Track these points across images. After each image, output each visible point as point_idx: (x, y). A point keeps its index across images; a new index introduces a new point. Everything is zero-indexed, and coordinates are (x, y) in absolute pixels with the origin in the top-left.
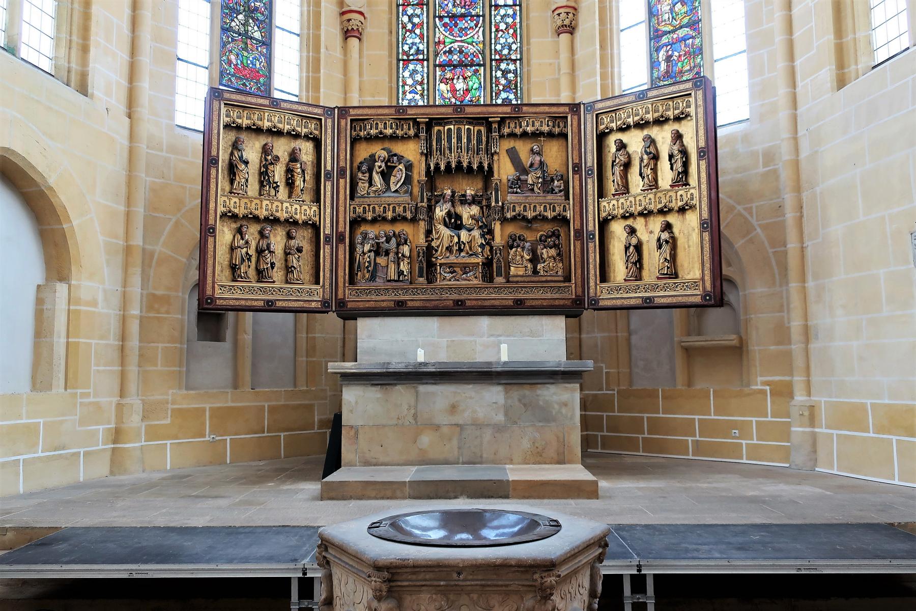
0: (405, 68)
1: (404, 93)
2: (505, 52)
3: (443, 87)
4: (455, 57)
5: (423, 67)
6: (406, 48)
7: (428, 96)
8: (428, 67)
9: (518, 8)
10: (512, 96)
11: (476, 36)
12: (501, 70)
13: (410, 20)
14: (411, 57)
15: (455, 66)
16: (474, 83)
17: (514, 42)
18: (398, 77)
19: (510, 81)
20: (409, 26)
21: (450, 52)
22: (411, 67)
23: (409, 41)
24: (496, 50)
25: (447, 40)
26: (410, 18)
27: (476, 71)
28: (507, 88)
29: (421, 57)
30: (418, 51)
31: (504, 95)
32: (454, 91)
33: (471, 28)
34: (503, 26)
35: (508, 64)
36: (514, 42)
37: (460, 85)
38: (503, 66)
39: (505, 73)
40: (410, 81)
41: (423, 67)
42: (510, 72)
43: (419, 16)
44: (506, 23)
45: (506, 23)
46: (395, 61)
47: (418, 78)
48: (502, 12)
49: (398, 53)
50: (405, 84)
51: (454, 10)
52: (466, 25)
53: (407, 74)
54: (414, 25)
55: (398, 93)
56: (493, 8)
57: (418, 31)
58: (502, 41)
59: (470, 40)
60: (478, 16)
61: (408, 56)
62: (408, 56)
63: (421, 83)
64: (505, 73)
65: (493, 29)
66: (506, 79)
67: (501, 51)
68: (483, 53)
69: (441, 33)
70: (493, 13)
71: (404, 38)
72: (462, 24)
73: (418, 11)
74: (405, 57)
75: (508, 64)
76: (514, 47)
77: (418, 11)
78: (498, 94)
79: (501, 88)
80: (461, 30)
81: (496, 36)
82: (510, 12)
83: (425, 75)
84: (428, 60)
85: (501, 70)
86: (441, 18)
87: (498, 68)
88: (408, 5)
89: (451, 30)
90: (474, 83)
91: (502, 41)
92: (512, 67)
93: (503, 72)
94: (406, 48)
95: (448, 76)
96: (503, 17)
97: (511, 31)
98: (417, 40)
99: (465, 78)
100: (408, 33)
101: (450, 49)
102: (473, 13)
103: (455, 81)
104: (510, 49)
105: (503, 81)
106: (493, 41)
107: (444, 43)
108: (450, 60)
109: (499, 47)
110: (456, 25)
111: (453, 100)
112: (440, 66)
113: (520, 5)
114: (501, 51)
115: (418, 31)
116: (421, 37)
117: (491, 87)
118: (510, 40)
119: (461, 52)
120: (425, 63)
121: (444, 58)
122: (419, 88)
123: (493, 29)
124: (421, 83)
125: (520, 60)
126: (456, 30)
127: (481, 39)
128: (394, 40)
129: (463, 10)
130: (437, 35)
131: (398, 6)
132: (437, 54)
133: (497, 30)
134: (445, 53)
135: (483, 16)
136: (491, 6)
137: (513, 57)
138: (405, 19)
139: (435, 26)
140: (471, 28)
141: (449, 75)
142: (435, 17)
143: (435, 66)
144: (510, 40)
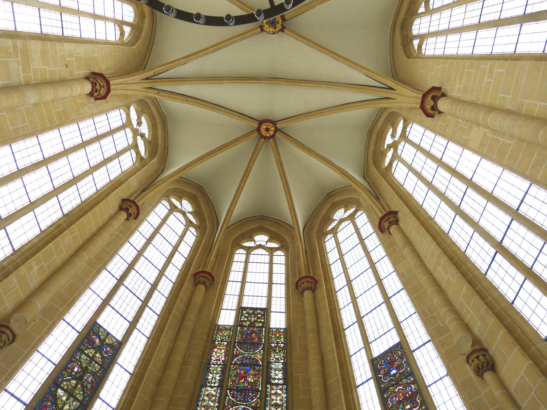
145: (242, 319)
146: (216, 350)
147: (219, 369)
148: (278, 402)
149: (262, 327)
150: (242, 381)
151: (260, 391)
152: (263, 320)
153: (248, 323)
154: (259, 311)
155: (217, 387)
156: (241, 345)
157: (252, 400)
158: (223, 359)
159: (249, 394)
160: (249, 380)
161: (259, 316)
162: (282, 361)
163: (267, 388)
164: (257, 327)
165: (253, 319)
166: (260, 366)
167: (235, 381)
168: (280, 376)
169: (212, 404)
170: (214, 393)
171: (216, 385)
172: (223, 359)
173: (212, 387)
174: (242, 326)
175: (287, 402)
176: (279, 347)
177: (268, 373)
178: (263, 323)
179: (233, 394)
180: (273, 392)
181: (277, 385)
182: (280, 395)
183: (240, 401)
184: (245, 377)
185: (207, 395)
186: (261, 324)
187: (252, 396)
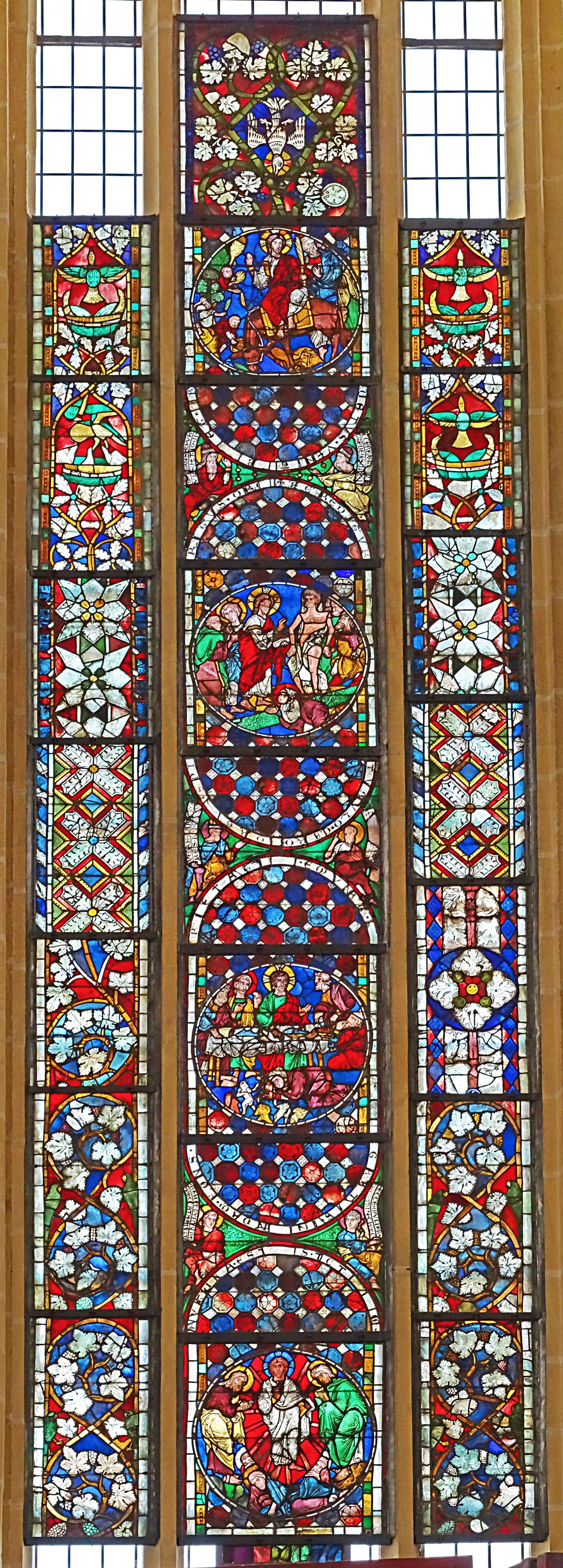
0: (59, 1347)
1: (54, 1446)
2: (473, 1285)
3: (215, 1423)
4: (268, 1303)
5: (132, 1343)
6: (63, 1263)
7: (154, 1460)
8: (154, 1343)
9: (524, 1108)
10: (500, 1465)
11: (352, 1222)
12: (454, 1358)
13: (80, 1153)
14: (84, 1303)
15: (267, 1342)
16: (343, 1410)
17: (508, 1247)
18: (30, 1384)
19: (489, 1405)
20: (78, 1178)
21: (245, 1281)
22: (84, 1342)
23: (78, 1237)
24: (433, 1275)
25: (232, 1234)
26: (82, 1140)
27: (355, 1361)
28: (480, 1434)
29: (124, 1302)
30: (114, 1280)
31: (466, 1461)
32: (258, 1439)
33: (333, 1187)
34: (462, 1182)
35: (483, 1336)
36: (508, 1247)
37: (285, 1420)
38: (464, 1343)
39: (472, 1369)
40: (78, 1402)
41: (132, 1343)
42: (492, 1365)
43: (114, 1137)
44: (477, 1170)
45: (477, 1170)
46: (20, 1320)
47: (114, 1387)
48: (461, 1123)
49: (30, 1285)
50: (56, 1410)
51: (263, 1111)
52: (312, 1175)
53: (65, 1371)
54: (96, 1171)
55: (30, 1448)
56: (423, 1108)
57: (112, 1199)
58: (461, 1239)
59: (325, 1236)
60: (363, 1140)
61: (71, 1301)
62: (71, 1301)
63: (125, 1409)
64: (472, 1369)
65: (424, 1192)
66: (476, 1392)
67: (456, 1280)
68: (381, 1287)
69: (208, 1206)
70: (422, 1125)
71: (55, 1224)
72: (297, 1171)
73: (113, 1116)
74: (59, 1303)
75: (483, 1336)
76: (508, 1264)
77: (113, 1116)
78: (443, 1453)
79: (455, 1429)
80: (290, 1192)
81: (435, 1220)
82: (493, 1123)
83: (143, 1376)
84: (153, 1315)
85: (454, 1358)
86: (208, 1146)
87: (443, 1351)
88: (70, 1092)
89: (249, 1194)
90: (343, 1410)
91: (461, 1239)
92: (499, 1347)
93: (463, 1363)
94: (63, 1263)
95: (235, 1382)
96: (463, 1142)
97: (497, 1203)
98: (110, 1233)
99: (306, 1391)
100: (71, 1205)
101: (245, 1268)
102: (342, 1125)
103: (264, 1404)
104: (492, 1273)
105: (464, 1405)
106: (423, 1242)
107: (219, 1245)
108: (245, 1316)
109: (445, 1265)
110: (270, 1173)
111: (258, 1480)
112: (198, 1338)
113: (534, 1098)
114: (456, 1280)
115: (112, 1199)
116: (126, 1217)
117: (417, 1427)
118: (494, 1237)
119: (289, 1281)
120: (143, 1325)
121: (220, 1306)
122: (115, 1427)
123: (424, 1192)
124: (125, 1409)
125: (531, 1317)
126: (270, 1193)
127: (373, 1229)
128: (20, 1232)
129: (300, 1114)
130: (193, 1213)
131: (31, 1092)
132: (189, 1290)
133: (442, 1195)
134: (223, 1285)
135: (383, 1138)
136: (414, 1098)
137: (505, 1308)
138: (61, 1147)
139: (184, 1178)
140: (333, 1187)
141: (240, 1378)
142: (184, 1139)
143: (184, 1339)
144: (494, 1237)
145: (203, 152)
146: (65, 456)
147: (116, 611)
148: (480, 817)
149: (344, 223)
150: (264, 686)
151: (373, 754)
152: (349, 153)
153: (249, 183)
154: (315, 54)
155: (126, 739)
156: (223, 398)
157: (332, 817)
158: (125, 526)
159: (310, 780)
160: (305, 675)
161: (322, 103)
162: (495, 521)
163: (410, 727)
164: (317, 226)
165: (278, 141)
166: (357, 567)
167: (223, 694)
168: (488, 638)
169: (115, 859)
170: (114, 786)
171: (116, 727)
172: (125, 526)
173: (93, 745)
174: (210, 220)
175: (529, 818)
176: (475, 402)
177: (416, 617)
178: (351, 176)
179: (224, 784)
180: (449, 754)
181: (471, 701)
182: (488, 772)
183: (265, 826)
184: (276, 658)
185: (77, 801)
186: (337, 194)
187: (332, 788)
